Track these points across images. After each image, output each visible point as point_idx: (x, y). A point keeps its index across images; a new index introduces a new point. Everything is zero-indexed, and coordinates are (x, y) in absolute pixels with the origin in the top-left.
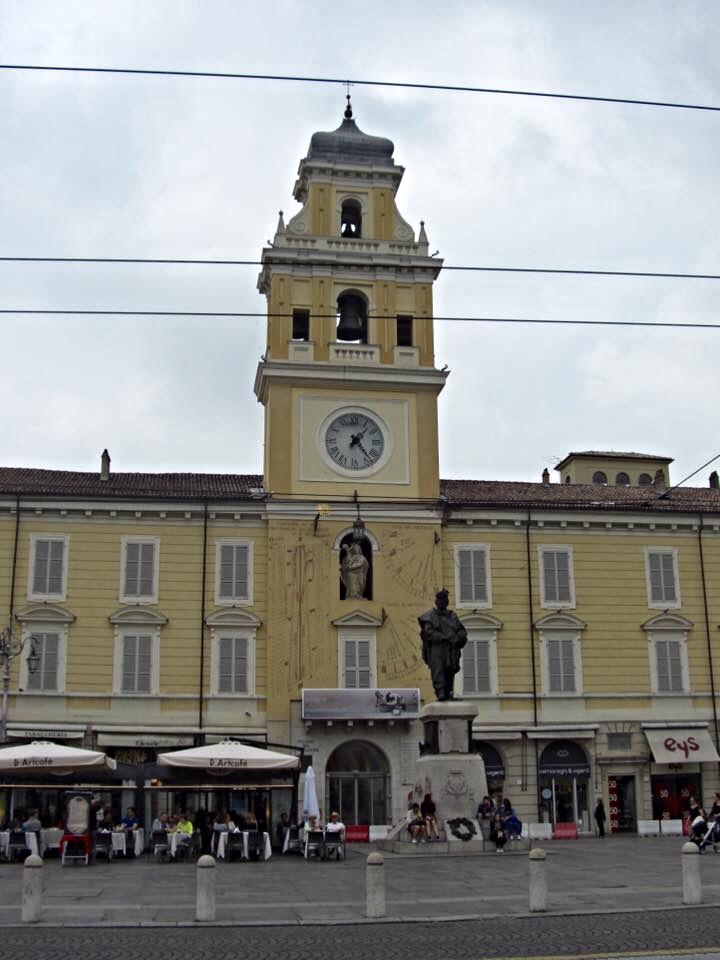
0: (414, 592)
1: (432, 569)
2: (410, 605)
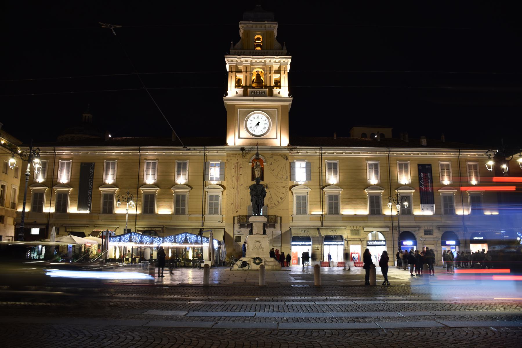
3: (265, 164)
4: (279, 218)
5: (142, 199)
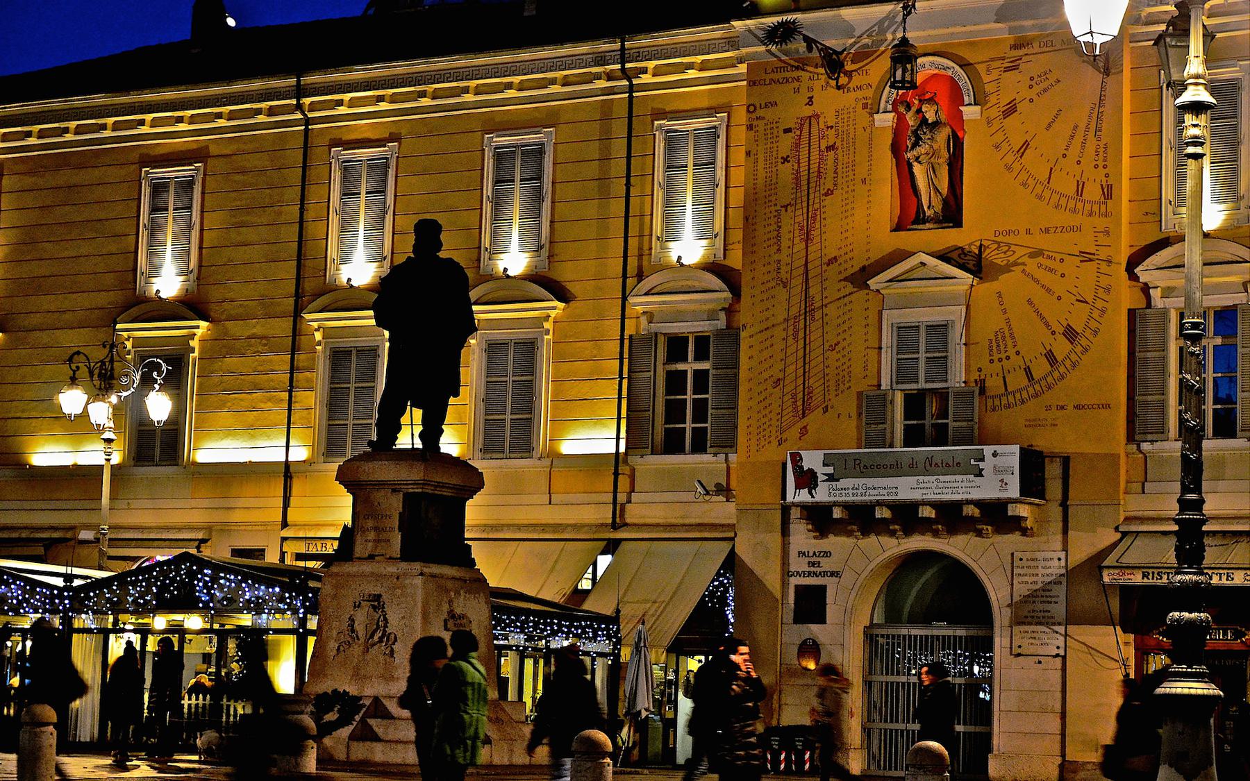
0: (1055, 197)
1: (1099, 139)
2: (1047, 231)
3: (970, 112)
4: (1053, 470)
5: (320, 375)
